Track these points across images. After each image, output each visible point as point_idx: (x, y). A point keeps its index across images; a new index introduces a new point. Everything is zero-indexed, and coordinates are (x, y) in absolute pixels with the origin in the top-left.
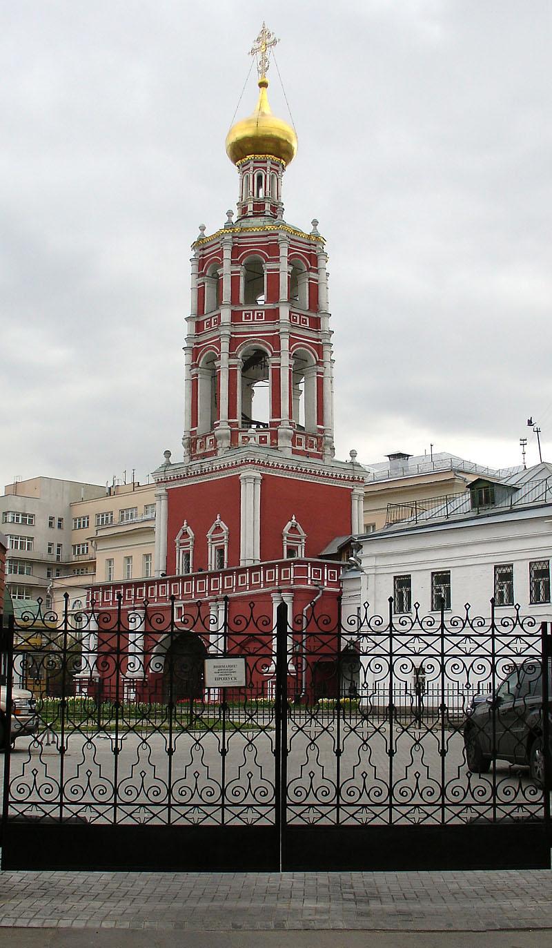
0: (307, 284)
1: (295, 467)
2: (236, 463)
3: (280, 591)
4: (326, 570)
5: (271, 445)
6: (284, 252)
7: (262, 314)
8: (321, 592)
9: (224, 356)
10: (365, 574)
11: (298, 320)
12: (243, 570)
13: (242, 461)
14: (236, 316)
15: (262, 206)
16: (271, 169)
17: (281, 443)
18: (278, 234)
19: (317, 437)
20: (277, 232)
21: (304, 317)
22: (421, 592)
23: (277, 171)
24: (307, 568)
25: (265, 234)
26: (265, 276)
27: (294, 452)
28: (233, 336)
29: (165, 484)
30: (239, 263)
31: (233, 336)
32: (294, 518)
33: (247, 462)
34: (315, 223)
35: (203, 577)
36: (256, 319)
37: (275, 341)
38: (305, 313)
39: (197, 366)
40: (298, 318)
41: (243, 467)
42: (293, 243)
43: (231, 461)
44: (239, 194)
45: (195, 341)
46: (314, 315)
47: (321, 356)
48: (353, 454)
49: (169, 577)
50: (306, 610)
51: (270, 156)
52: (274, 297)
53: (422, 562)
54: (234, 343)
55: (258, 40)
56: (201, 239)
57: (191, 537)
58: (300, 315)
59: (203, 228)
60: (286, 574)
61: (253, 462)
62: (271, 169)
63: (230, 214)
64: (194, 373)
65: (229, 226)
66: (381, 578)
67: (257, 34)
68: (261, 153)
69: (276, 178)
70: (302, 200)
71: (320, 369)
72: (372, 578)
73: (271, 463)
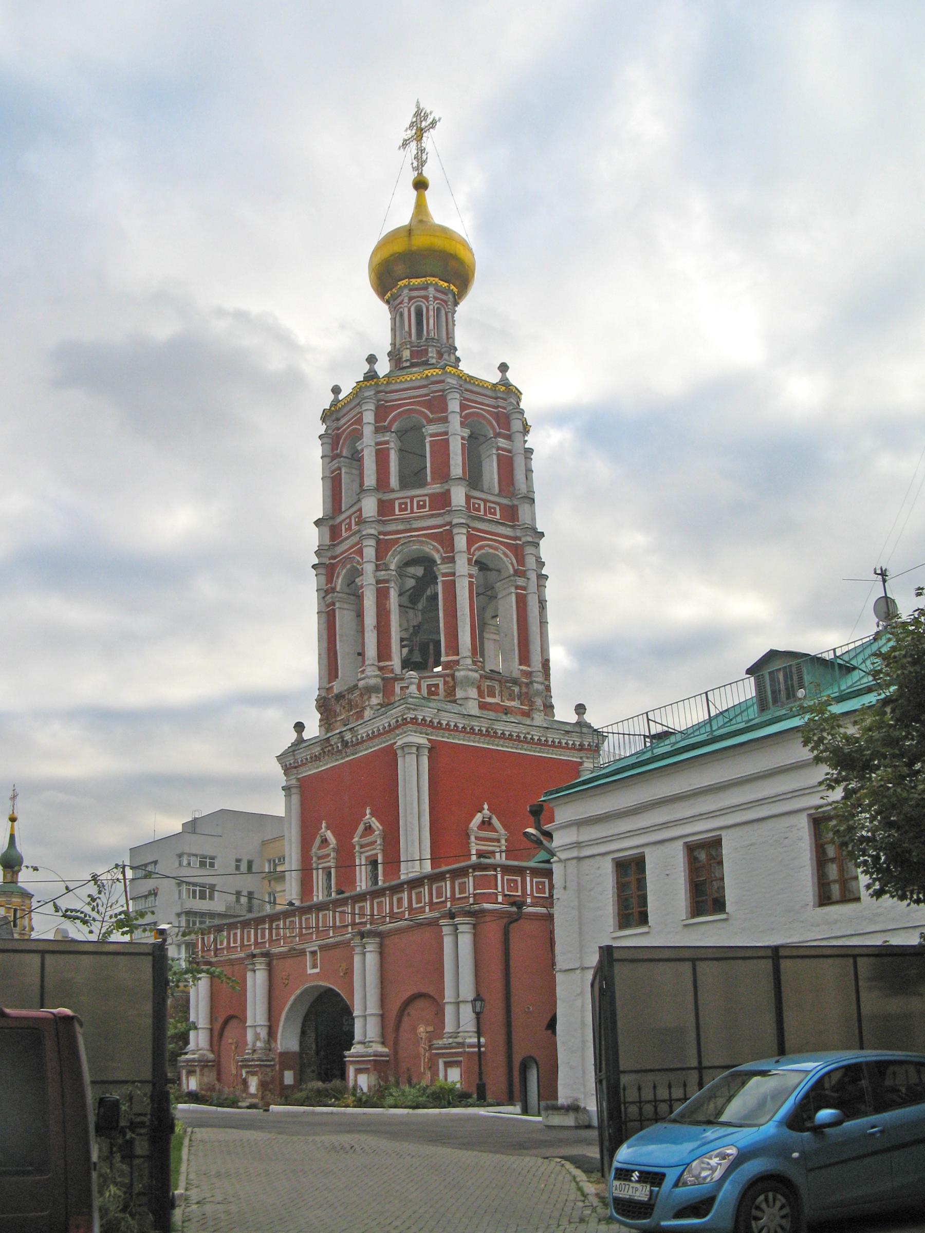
0: (495, 457)
1: (484, 729)
2: (390, 725)
4: (528, 879)
7: (425, 501)
9: (369, 568)
10: (560, 861)
13: (397, 721)
14: (385, 508)
16: (436, 298)
17: (459, 694)
20: (442, 378)
21: (493, 505)
23: (446, 302)
24: (496, 876)
25: (424, 383)
26: (428, 445)
27: (483, 706)
28: (381, 537)
29: (295, 771)
30: (387, 429)
31: (381, 537)
32: (486, 807)
33: (405, 722)
34: (503, 368)
36: (415, 510)
38: (491, 498)
39: (333, 590)
41: (397, 732)
42: (468, 395)
43: (383, 722)
44: (388, 340)
45: (329, 554)
46: (505, 501)
47: (521, 560)
48: (580, 709)
51: (432, 279)
52: (443, 474)
54: (382, 548)
55: (412, 125)
58: (485, 501)
59: (336, 390)
60: (463, 889)
61: (414, 721)
62: (436, 298)
63: (372, 359)
65: (371, 376)
67: (409, 118)
69: (443, 312)
71: (521, 582)
73: (444, 723)
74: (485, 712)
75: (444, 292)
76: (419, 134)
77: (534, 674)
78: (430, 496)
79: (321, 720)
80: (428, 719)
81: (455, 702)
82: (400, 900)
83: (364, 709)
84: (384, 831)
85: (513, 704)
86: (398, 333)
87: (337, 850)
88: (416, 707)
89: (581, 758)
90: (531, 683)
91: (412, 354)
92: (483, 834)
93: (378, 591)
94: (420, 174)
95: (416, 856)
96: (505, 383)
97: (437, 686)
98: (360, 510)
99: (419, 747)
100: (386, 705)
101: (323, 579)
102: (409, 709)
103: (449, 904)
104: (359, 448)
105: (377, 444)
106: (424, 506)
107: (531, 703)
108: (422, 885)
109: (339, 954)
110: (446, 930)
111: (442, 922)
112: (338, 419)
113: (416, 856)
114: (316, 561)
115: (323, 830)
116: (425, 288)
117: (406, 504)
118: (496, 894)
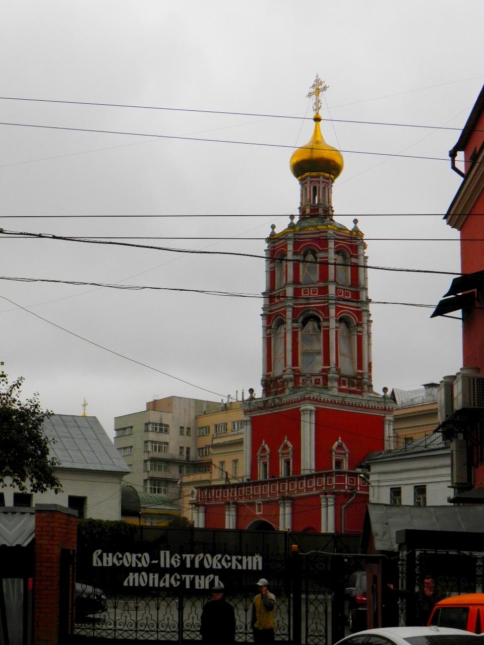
1: (340, 402)
2: (298, 399)
3: (326, 494)
5: (323, 385)
6: (331, 244)
7: (316, 290)
8: (355, 495)
9: (289, 322)
11: (343, 294)
12: (301, 478)
13: (301, 398)
15: (316, 210)
16: (323, 182)
17: (330, 384)
18: (326, 232)
19: (357, 379)
22: (408, 497)
24: (345, 477)
27: (340, 390)
28: (295, 306)
29: (249, 413)
31: (295, 306)
32: (340, 438)
33: (305, 399)
35: (275, 481)
37: (326, 310)
38: (348, 288)
40: (343, 292)
41: (301, 403)
45: (269, 309)
46: (354, 289)
47: (360, 318)
49: (253, 481)
50: (344, 508)
53: (408, 479)
55: (314, 86)
56: (273, 234)
57: (267, 452)
58: (344, 290)
59: (273, 227)
60: (330, 481)
61: (309, 398)
64: (269, 333)
65: (291, 226)
66: (382, 489)
67: (312, 83)
68: (317, 170)
69: (327, 189)
70: (346, 202)
71: (359, 329)
72: (376, 488)
73: (322, 399)
74: (341, 393)
75: (328, 179)
76: (318, 91)
77: (365, 374)
78: (319, 287)
79: (263, 390)
80: (315, 398)
81: (327, 388)
82: (302, 484)
83: (285, 389)
84: (293, 448)
85: (354, 389)
86: (304, 198)
88: (311, 392)
89: (385, 414)
90: (363, 378)
91: (311, 211)
92: (339, 451)
93: (293, 332)
94: (317, 114)
95: (308, 461)
96: (356, 230)
97: (319, 380)
98: (285, 291)
99: (311, 411)
100: (296, 386)
101: (265, 321)
102: (307, 393)
103: (324, 488)
106: (315, 292)
107: (362, 388)
108: (313, 478)
109: (272, 505)
110: (323, 500)
111: (321, 496)
112: (274, 243)
113: (308, 461)
114: (262, 312)
115: (263, 444)
116: (318, 177)
117: (307, 290)
118: (345, 485)
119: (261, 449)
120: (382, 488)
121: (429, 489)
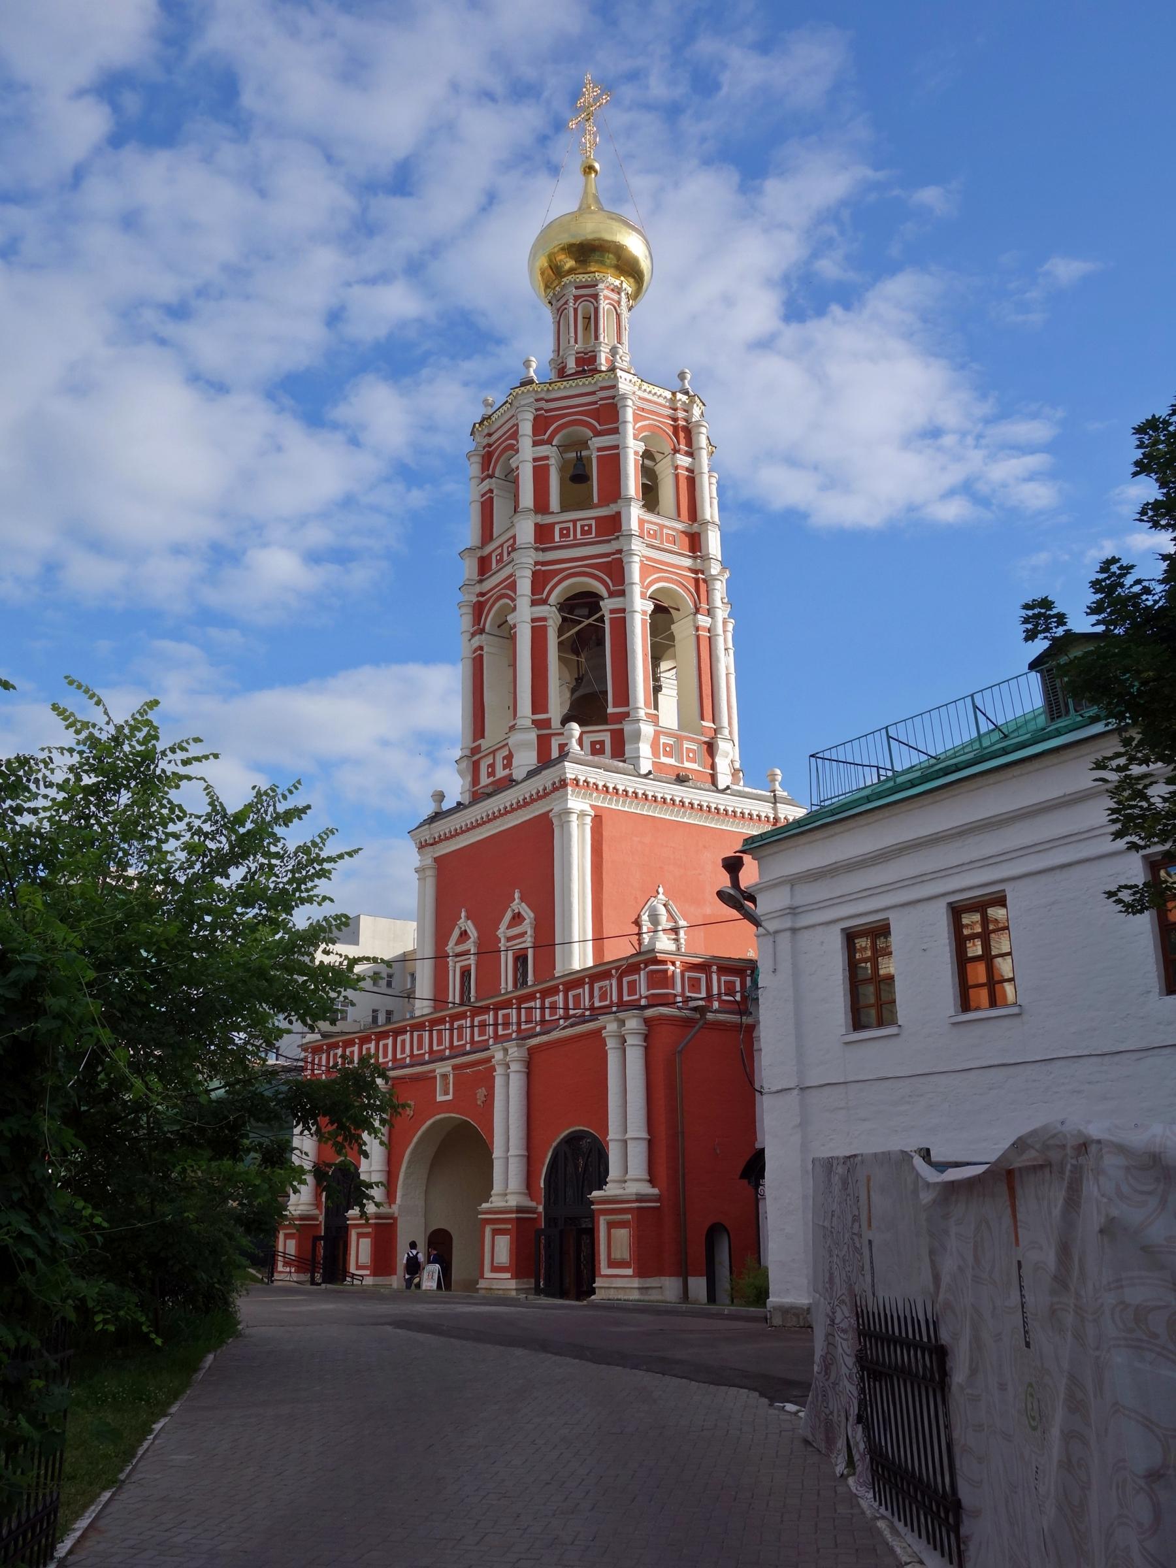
4: (715, 977)
14: (543, 534)
30: (549, 442)
36: (579, 536)
53: (919, 879)
54: (540, 581)
57: (472, 940)
87: (480, 943)
91: (579, 361)
97: (602, 743)
98: (514, 537)
104: (514, 466)
105: (535, 460)
106: (589, 532)
117: (568, 529)
119: (456, 933)
120: (805, 935)
121: (1017, 912)
